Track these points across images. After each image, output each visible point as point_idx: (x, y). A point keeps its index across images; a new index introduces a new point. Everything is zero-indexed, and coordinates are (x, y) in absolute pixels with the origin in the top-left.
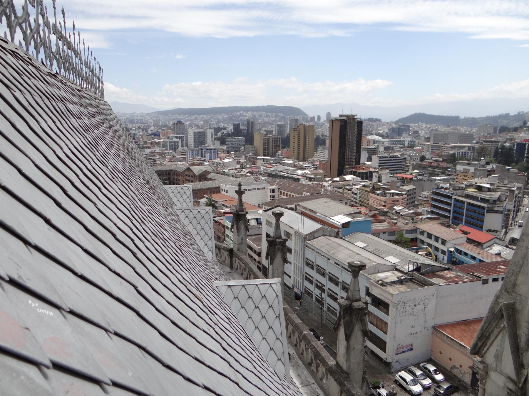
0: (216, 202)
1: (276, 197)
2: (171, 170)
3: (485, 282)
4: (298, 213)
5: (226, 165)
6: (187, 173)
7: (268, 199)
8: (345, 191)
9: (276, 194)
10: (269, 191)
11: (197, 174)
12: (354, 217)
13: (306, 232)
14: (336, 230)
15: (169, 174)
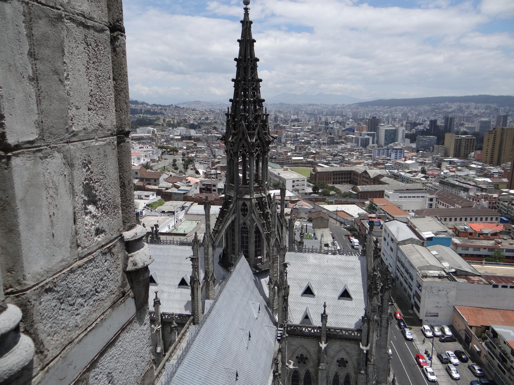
0: (377, 206)
1: (434, 206)
2: (352, 171)
3: (495, 286)
4: (408, 226)
5: (407, 166)
6: (364, 175)
7: (427, 207)
8: (510, 205)
9: (434, 202)
10: (427, 199)
11: (372, 177)
12: (436, 234)
13: (400, 239)
14: (422, 241)
15: (350, 174)
